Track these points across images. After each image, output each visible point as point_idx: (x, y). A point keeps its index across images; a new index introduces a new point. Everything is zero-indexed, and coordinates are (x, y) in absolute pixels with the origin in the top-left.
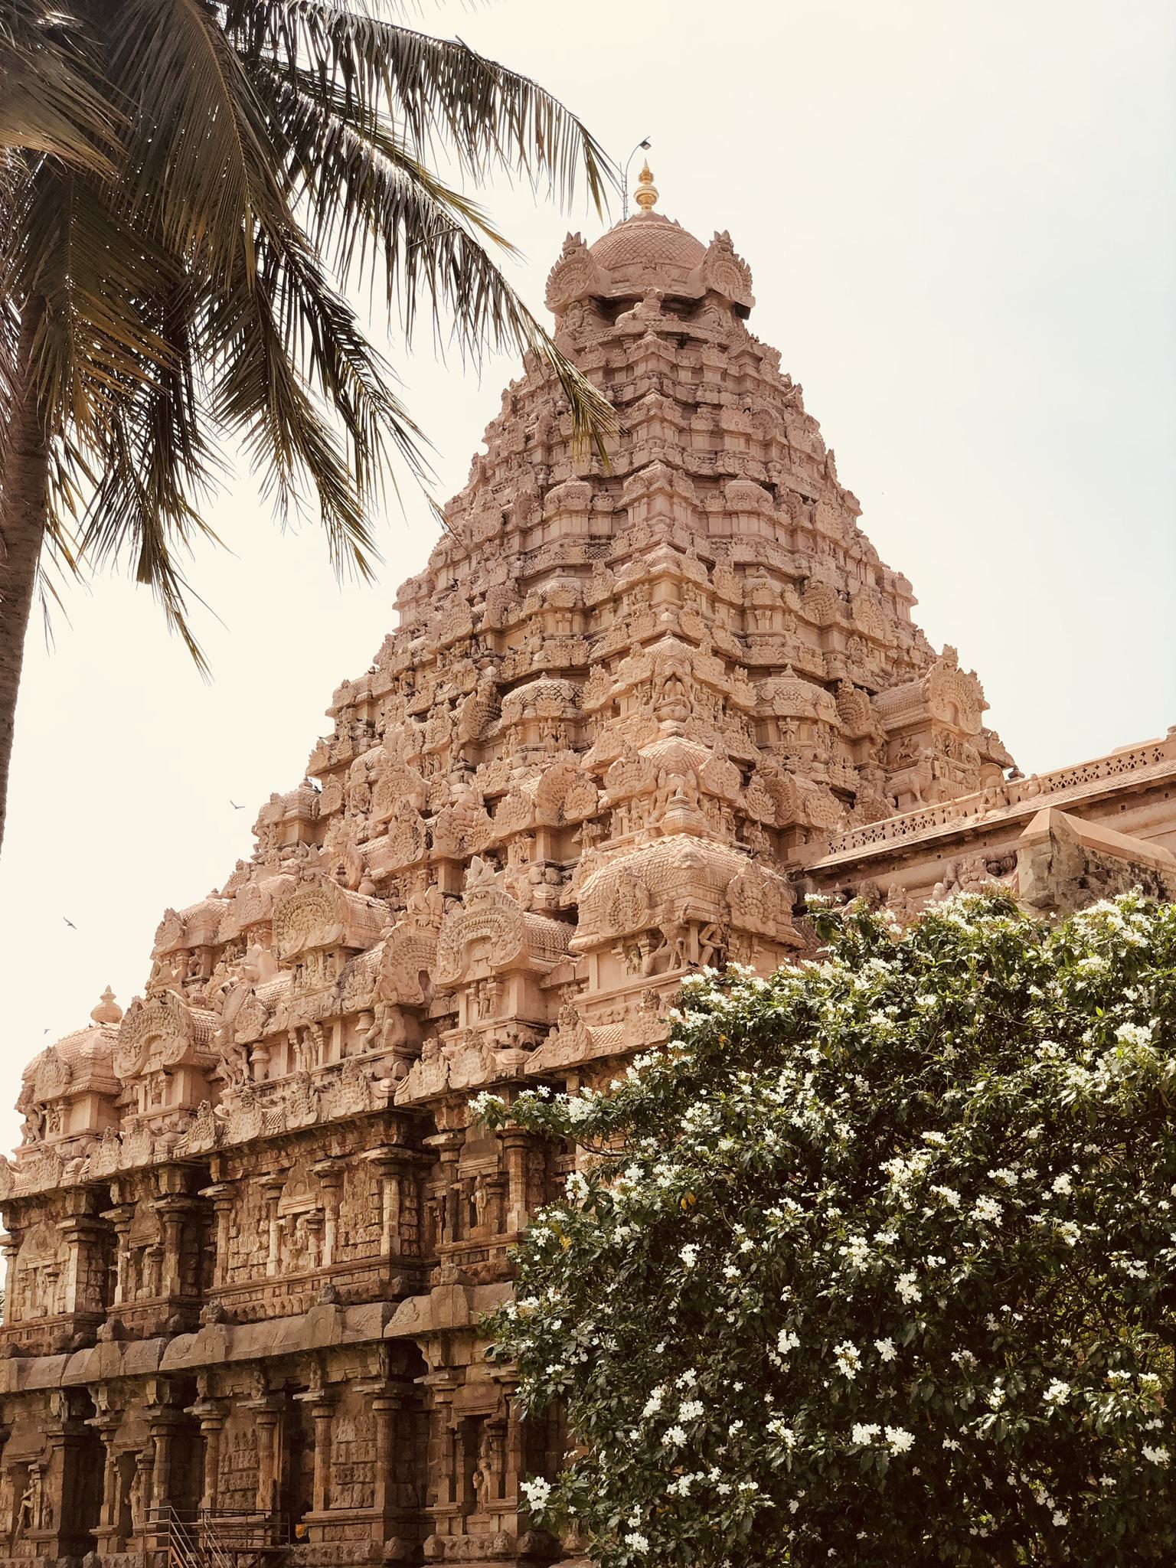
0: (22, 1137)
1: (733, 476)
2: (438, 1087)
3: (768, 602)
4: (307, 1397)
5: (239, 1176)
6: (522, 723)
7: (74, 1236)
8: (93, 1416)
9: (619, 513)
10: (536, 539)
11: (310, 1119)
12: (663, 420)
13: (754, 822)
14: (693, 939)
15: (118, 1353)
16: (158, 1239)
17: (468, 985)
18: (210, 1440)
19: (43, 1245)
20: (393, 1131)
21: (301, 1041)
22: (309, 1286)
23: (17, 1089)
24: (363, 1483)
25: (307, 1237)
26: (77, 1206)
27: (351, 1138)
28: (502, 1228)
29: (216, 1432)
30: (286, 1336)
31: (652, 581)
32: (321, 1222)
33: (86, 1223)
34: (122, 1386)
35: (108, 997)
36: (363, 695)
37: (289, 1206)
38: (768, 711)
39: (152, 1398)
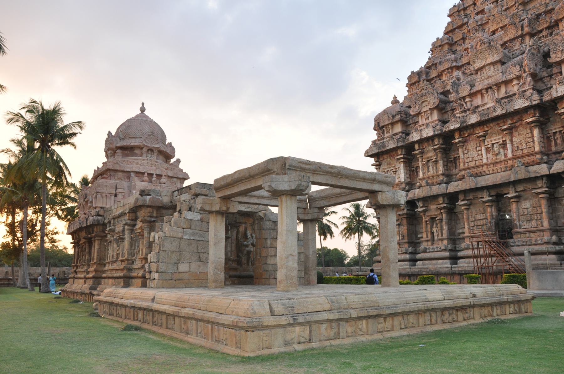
5: (466, 136)
7: (402, 160)
8: (417, 208)
11: (504, 112)
15: (429, 189)
16: (435, 157)
18: (465, 212)
19: (389, 164)
20: (537, 112)
21: (487, 92)
22: (503, 164)
23: (373, 125)
24: (536, 220)
25: (499, 149)
26: (402, 152)
27: (516, 118)
30: (502, 178)
33: (405, 156)
35: (395, 97)
37: (491, 141)
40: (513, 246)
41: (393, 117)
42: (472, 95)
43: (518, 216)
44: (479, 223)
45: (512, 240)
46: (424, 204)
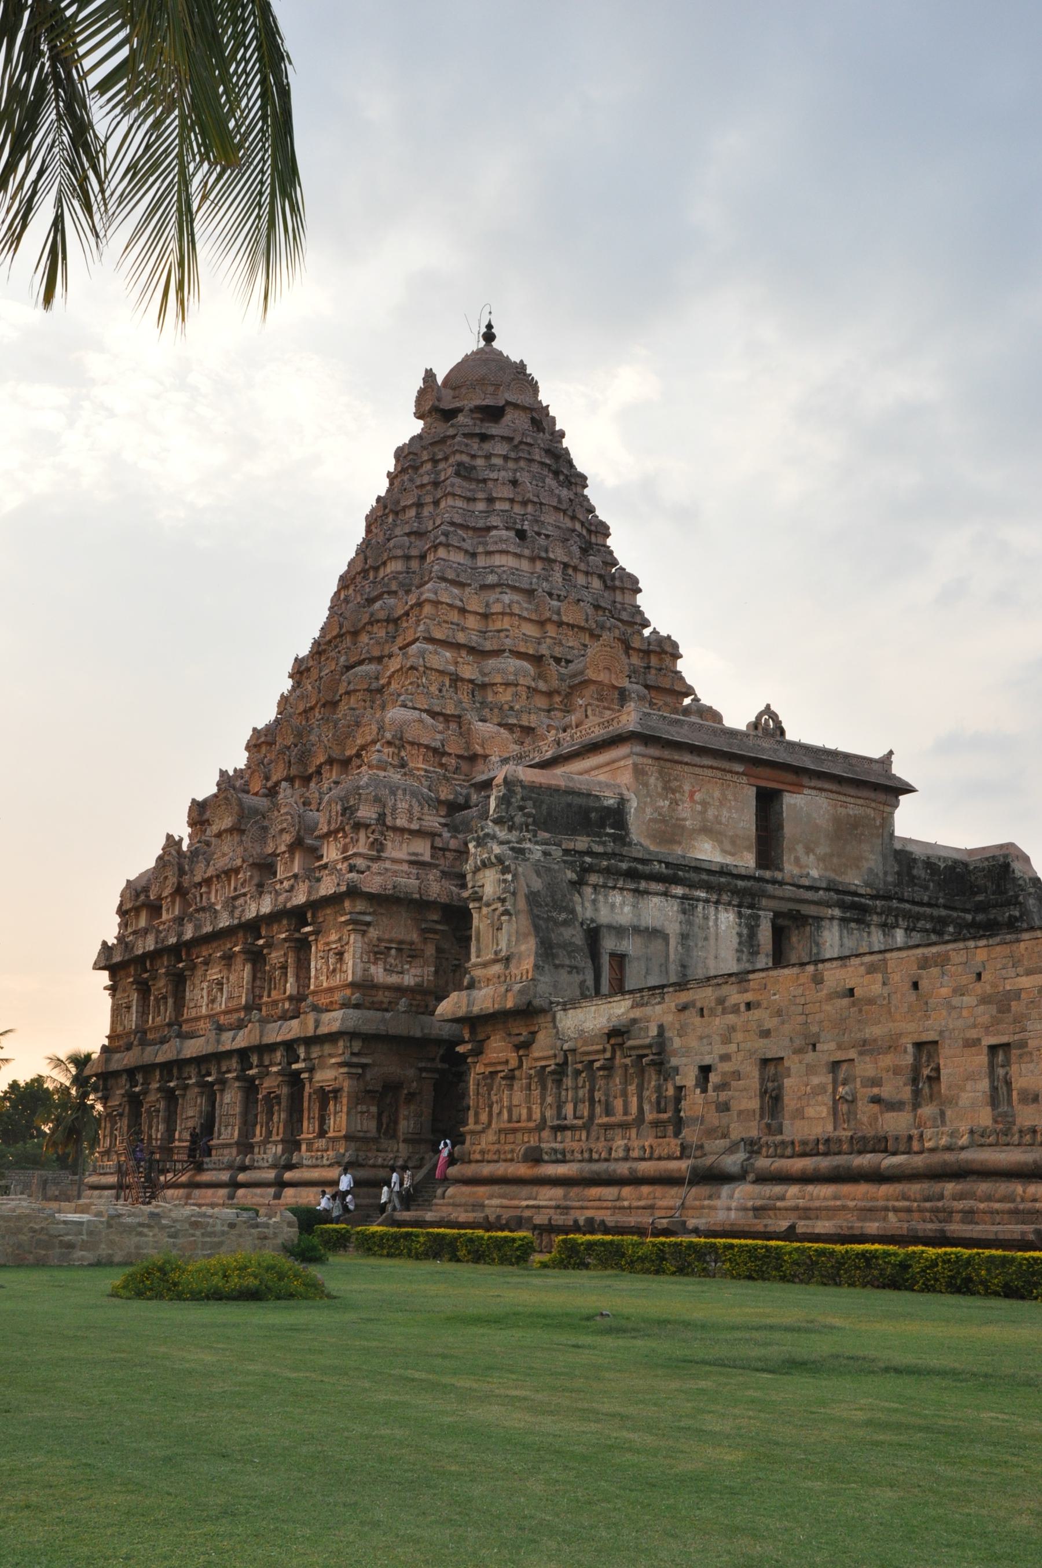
0: (117, 930)
1: (496, 528)
2: (254, 915)
3: (500, 610)
4: (210, 1079)
6: (348, 693)
7: (134, 987)
9: (423, 557)
10: (381, 574)
12: (454, 495)
13: (450, 754)
14: (362, 835)
17: (278, 855)
18: (180, 1101)
19: (124, 991)
23: (117, 901)
28: (285, 993)
29: (184, 1096)
31: (419, 605)
32: (222, 984)
34: (147, 1069)
36: (303, 667)
37: (211, 975)
38: (486, 680)
39: (158, 1077)
40: (208, 1170)
41: (137, 896)
42: (208, 881)
43: (221, 1116)
44: (190, 1124)
45: (207, 1160)
46: (145, 1079)
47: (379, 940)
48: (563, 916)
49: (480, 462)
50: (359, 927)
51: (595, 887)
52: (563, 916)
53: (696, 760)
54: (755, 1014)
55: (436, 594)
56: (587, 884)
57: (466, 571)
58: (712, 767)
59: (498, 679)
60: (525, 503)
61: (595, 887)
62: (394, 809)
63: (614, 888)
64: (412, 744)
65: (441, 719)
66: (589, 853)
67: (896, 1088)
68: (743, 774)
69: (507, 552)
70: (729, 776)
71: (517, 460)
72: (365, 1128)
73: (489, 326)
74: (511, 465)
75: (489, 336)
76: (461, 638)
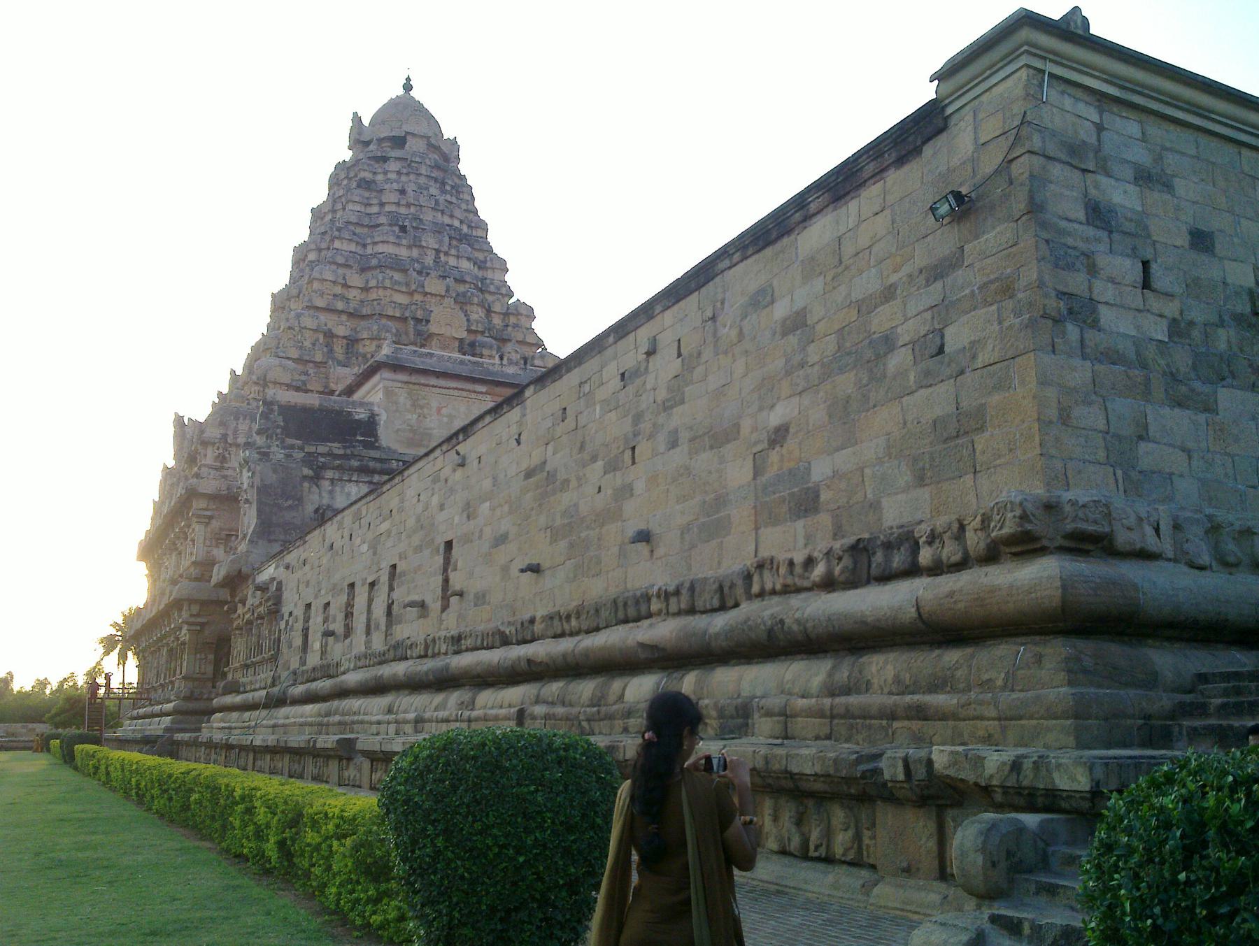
47: (221, 529)
48: (290, 502)
49: (380, 177)
50: (203, 520)
51: (332, 480)
52: (290, 502)
53: (442, 382)
54: (307, 567)
55: (321, 273)
56: (323, 478)
57: (354, 257)
58: (456, 389)
59: (365, 336)
60: (408, 205)
61: (332, 480)
62: (236, 431)
63: (350, 481)
64: (275, 383)
65: (311, 365)
66: (330, 454)
67: (338, 626)
68: (486, 393)
69: (388, 242)
70: (473, 395)
71: (407, 174)
72: (203, 670)
73: (408, 79)
74: (404, 178)
75: (408, 87)
76: (340, 305)
